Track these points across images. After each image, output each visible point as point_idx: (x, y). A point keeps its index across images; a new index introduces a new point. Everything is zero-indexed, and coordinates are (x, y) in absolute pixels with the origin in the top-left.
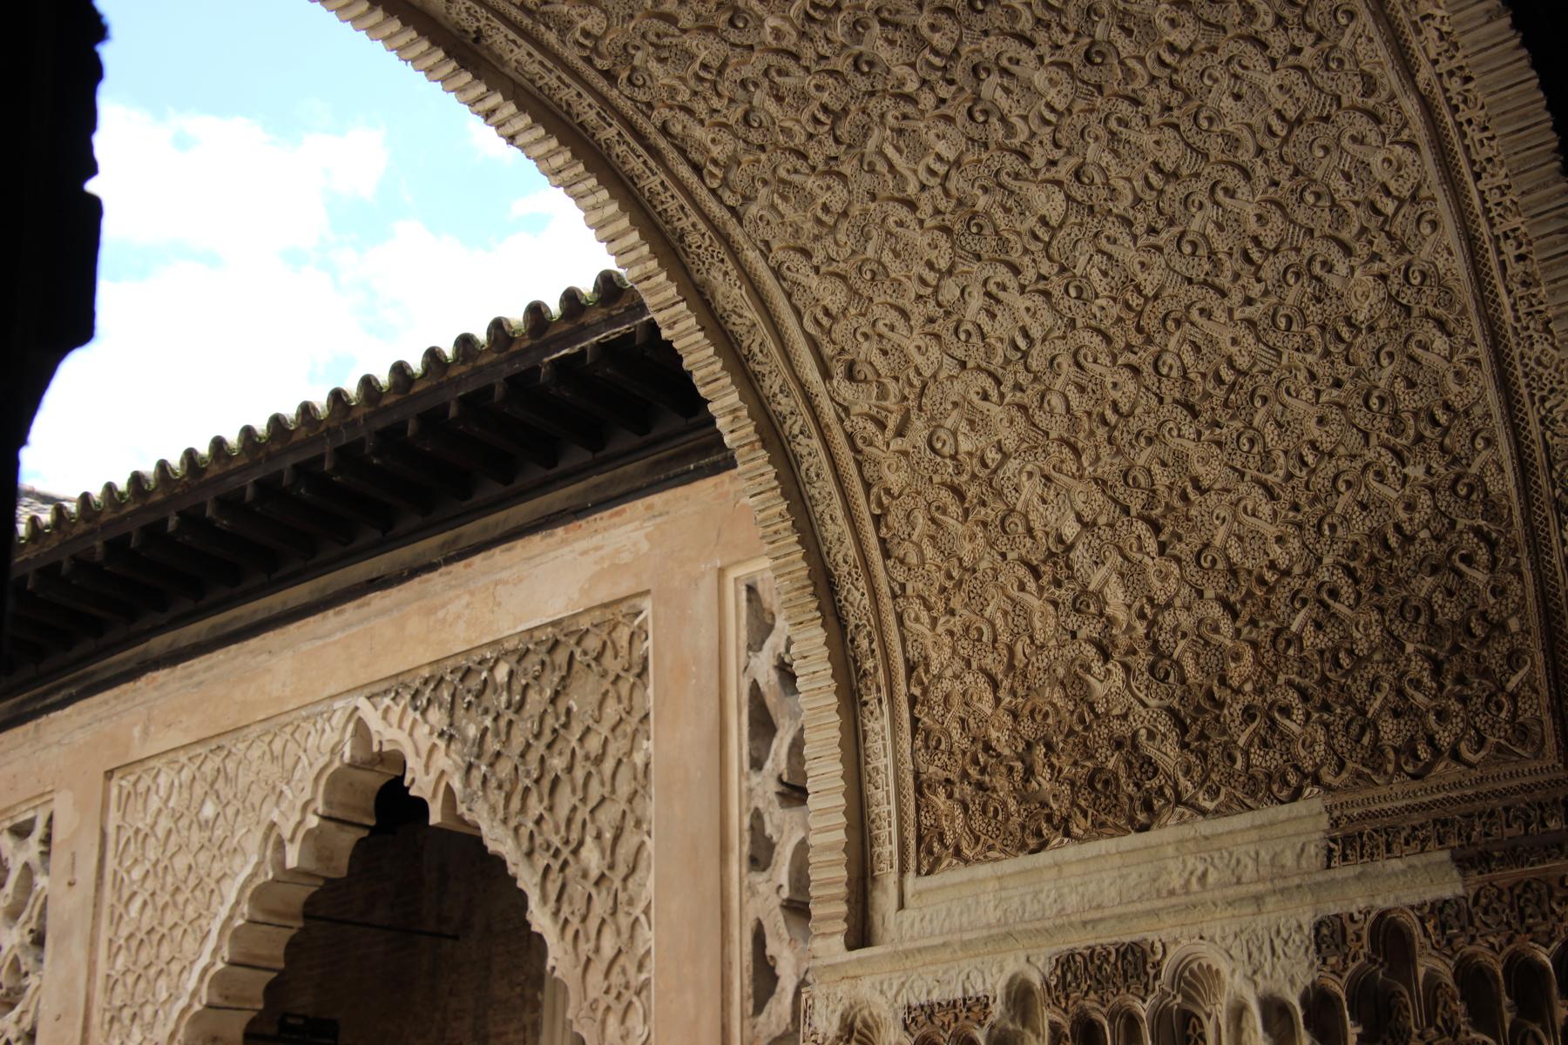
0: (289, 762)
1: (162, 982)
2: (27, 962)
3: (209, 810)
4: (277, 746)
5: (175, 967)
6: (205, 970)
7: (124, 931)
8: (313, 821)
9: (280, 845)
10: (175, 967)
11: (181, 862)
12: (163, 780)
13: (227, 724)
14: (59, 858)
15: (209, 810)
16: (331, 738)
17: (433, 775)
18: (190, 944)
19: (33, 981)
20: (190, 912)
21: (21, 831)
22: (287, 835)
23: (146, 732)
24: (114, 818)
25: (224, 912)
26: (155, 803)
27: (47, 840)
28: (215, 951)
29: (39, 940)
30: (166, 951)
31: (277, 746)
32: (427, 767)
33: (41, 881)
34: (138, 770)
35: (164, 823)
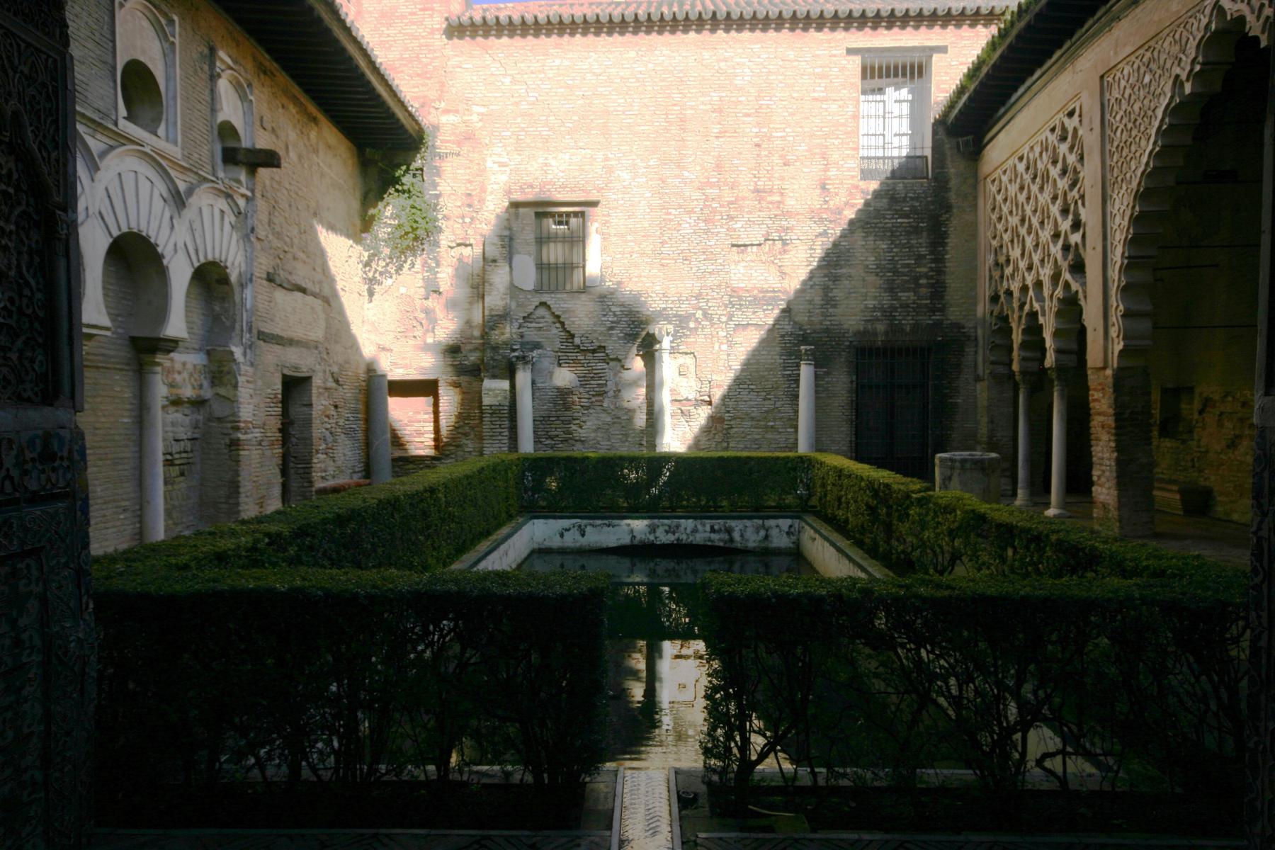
0: (1183, 42)
1: (1133, 163)
2: (1079, 167)
3: (1147, 79)
4: (1177, 36)
5: (1138, 154)
6: (1151, 152)
7: (1115, 144)
8: (1198, 68)
9: (1182, 84)
10: (1138, 154)
11: (1136, 107)
12: (1126, 72)
13: (1152, 34)
14: (1085, 120)
15: (1147, 79)
16: (1205, 21)
17: (1262, 20)
18: (1143, 143)
19: (1081, 175)
20: (1142, 128)
21: (1071, 114)
22: (1184, 77)
23: (1116, 53)
24: (1107, 96)
25: (1156, 124)
26: (1123, 83)
27: (1080, 116)
28: (1155, 143)
29: (1081, 158)
30: (1133, 148)
31: (1177, 36)
32: (1258, 18)
33: (1080, 132)
34: (1114, 71)
35: (1128, 91)
